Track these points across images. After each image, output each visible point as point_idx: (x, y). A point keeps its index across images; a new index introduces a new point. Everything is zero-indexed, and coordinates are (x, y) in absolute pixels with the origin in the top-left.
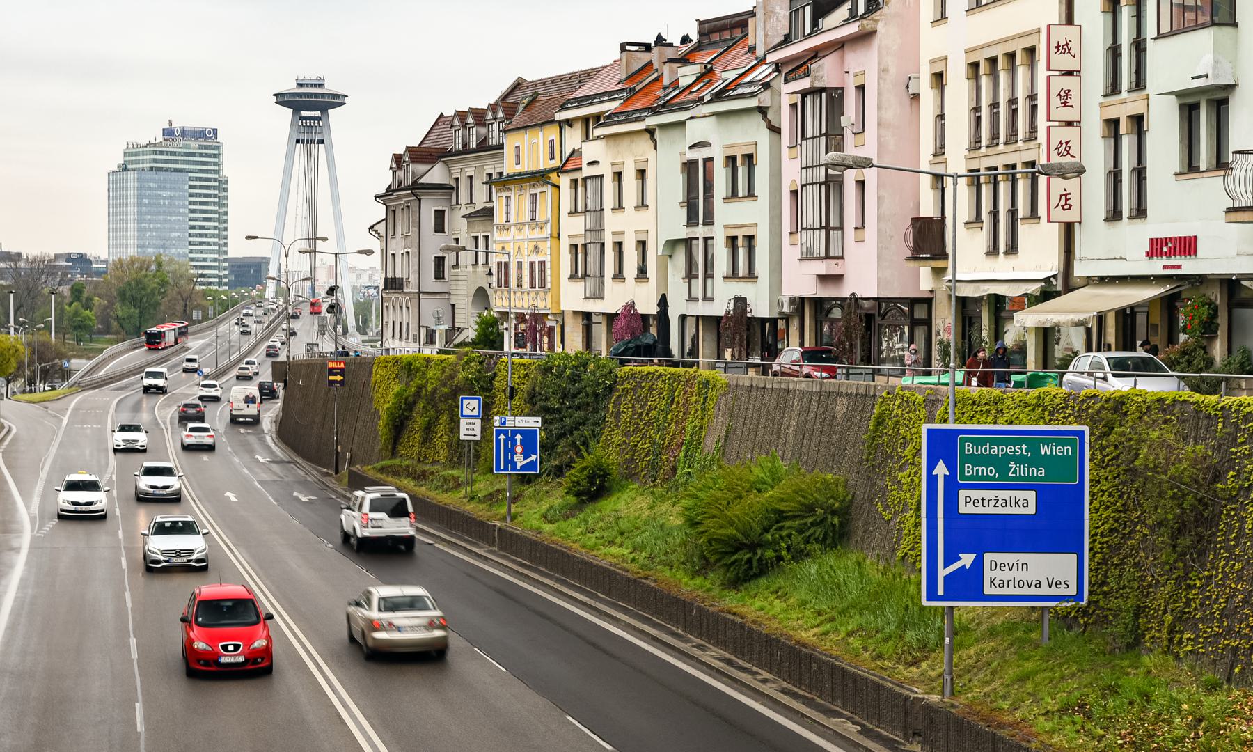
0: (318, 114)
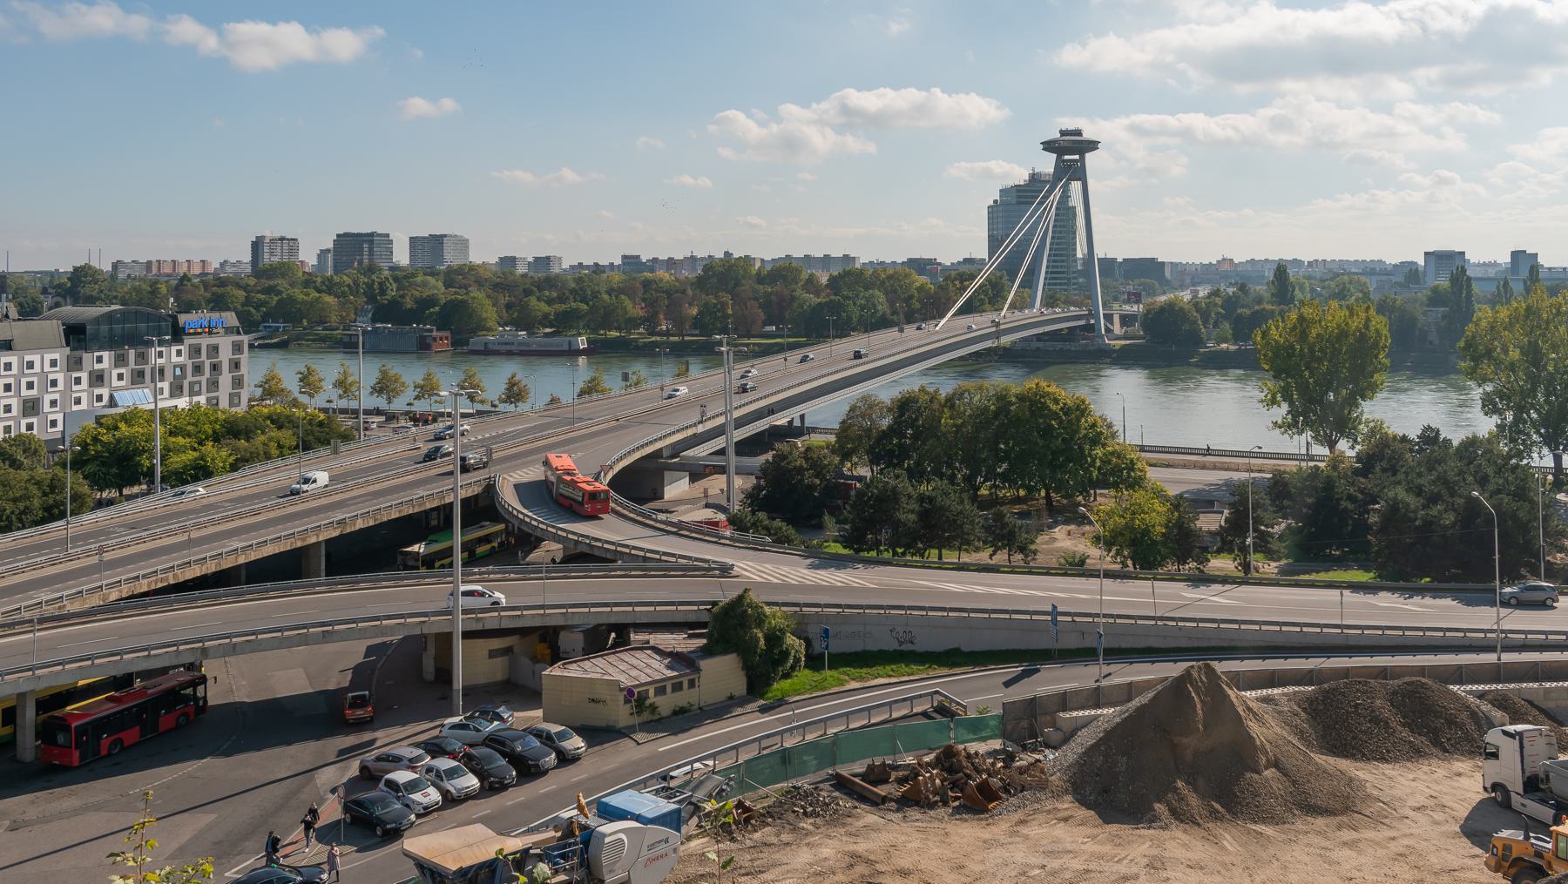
0: (1077, 157)
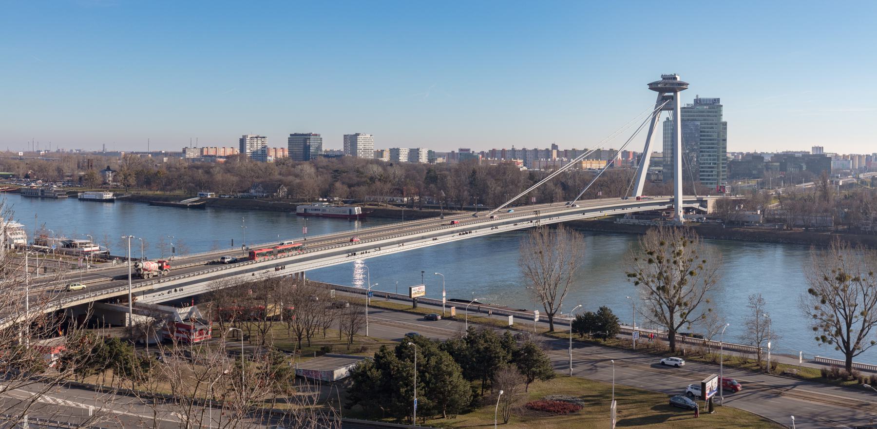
0: (672, 94)
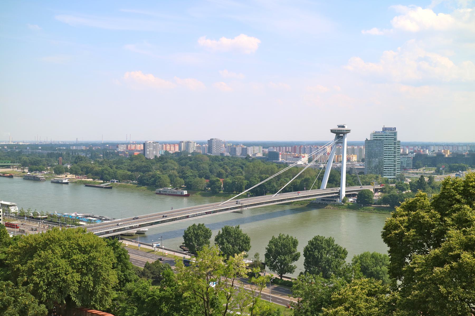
0: (342, 135)
